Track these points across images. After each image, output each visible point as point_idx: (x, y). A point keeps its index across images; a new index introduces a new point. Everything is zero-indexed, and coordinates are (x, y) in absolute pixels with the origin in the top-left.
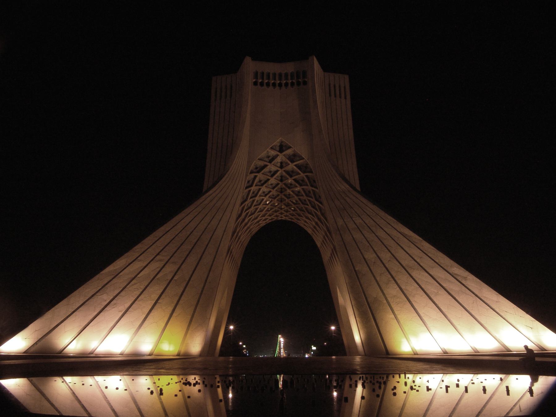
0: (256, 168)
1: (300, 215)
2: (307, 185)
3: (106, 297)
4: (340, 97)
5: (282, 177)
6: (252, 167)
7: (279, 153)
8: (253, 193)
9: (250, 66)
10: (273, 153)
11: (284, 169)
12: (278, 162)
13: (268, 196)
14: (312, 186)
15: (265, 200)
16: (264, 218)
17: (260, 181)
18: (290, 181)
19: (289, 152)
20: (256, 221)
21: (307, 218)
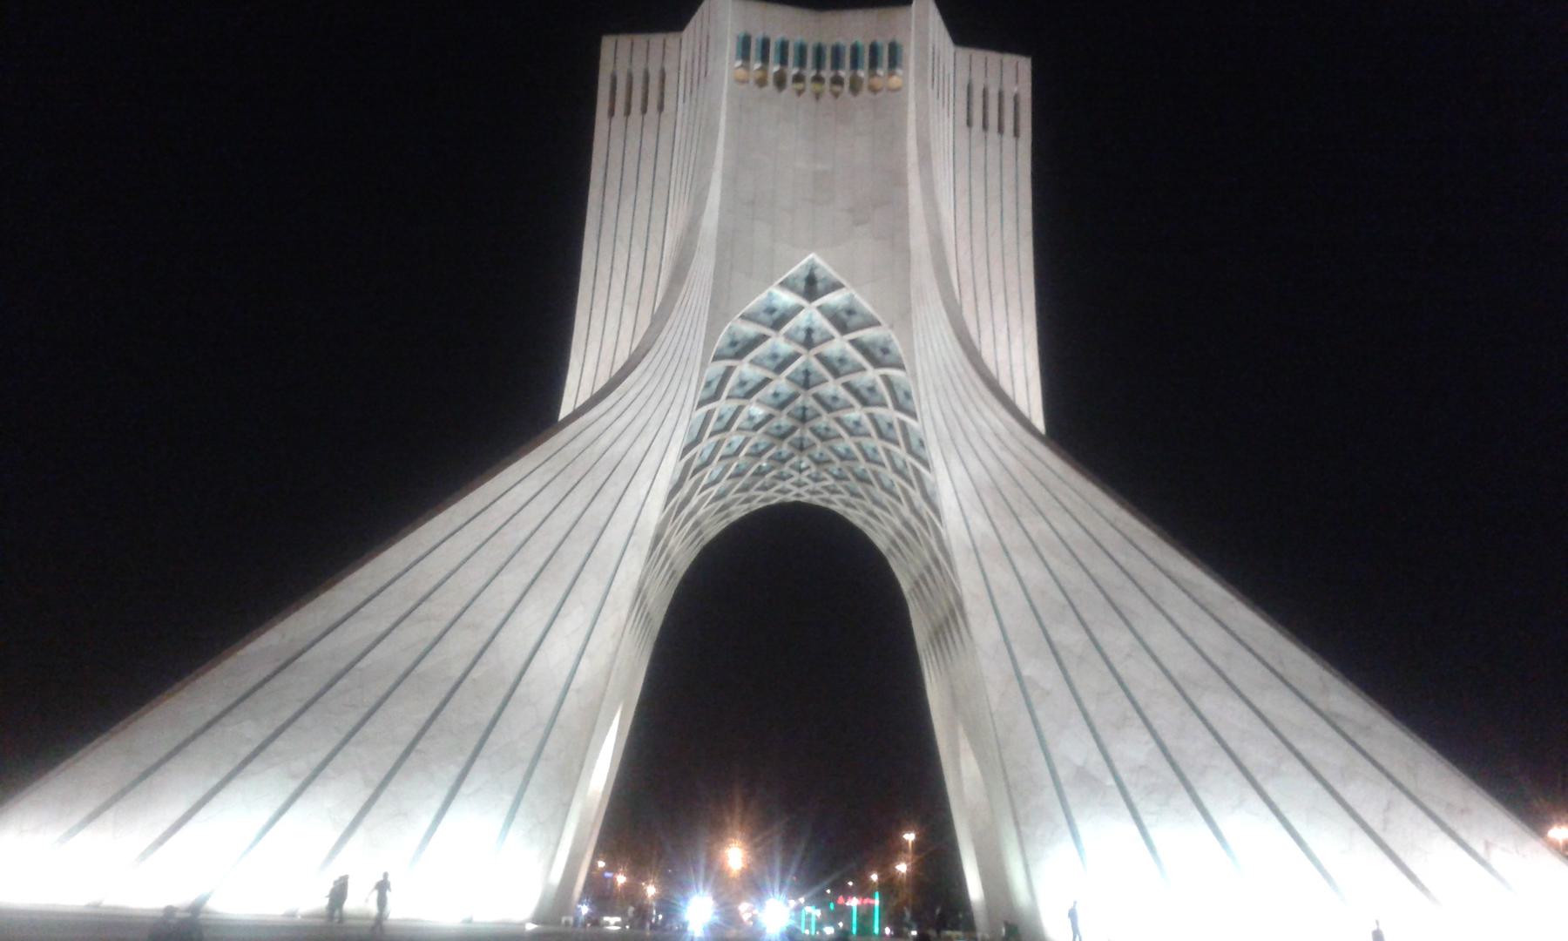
0: (733, 344)
1: (854, 494)
2: (884, 405)
4: (1001, 129)
5: (807, 373)
6: (722, 340)
7: (803, 302)
8: (720, 418)
10: (786, 299)
11: (815, 351)
12: (798, 328)
13: (760, 431)
14: (899, 407)
15: (751, 443)
16: (744, 496)
17: (742, 383)
18: (832, 387)
19: (834, 299)
21: (876, 502)
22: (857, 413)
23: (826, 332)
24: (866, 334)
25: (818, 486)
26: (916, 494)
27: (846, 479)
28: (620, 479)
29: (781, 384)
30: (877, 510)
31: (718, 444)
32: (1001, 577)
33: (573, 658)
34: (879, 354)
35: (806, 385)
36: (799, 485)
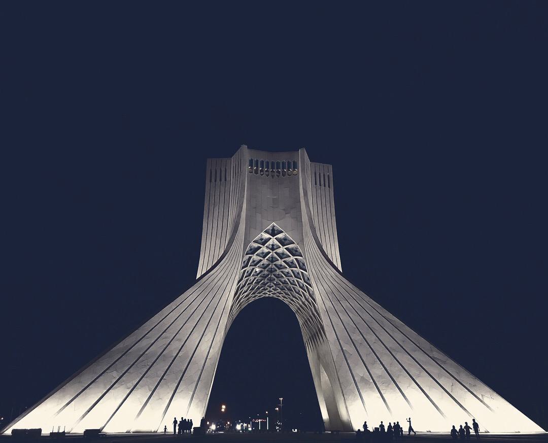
0: (251, 250)
1: (287, 294)
3: (116, 375)
4: (325, 186)
5: (272, 258)
7: (271, 237)
9: (246, 153)
10: (267, 236)
14: (301, 268)
16: (254, 295)
17: (254, 261)
18: (280, 262)
19: (280, 236)
20: (247, 298)
21: (294, 297)
22: (288, 270)
23: (278, 246)
24: (290, 246)
25: (275, 292)
26: (307, 294)
27: (285, 290)
28: (220, 292)
29: (265, 261)
30: (294, 299)
31: (247, 280)
32: (335, 319)
33: (208, 348)
34: (294, 252)
35: (272, 261)
36: (269, 292)
